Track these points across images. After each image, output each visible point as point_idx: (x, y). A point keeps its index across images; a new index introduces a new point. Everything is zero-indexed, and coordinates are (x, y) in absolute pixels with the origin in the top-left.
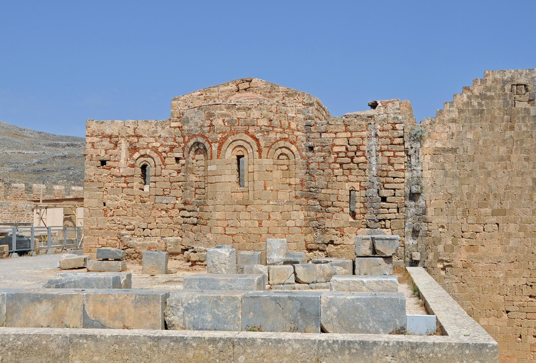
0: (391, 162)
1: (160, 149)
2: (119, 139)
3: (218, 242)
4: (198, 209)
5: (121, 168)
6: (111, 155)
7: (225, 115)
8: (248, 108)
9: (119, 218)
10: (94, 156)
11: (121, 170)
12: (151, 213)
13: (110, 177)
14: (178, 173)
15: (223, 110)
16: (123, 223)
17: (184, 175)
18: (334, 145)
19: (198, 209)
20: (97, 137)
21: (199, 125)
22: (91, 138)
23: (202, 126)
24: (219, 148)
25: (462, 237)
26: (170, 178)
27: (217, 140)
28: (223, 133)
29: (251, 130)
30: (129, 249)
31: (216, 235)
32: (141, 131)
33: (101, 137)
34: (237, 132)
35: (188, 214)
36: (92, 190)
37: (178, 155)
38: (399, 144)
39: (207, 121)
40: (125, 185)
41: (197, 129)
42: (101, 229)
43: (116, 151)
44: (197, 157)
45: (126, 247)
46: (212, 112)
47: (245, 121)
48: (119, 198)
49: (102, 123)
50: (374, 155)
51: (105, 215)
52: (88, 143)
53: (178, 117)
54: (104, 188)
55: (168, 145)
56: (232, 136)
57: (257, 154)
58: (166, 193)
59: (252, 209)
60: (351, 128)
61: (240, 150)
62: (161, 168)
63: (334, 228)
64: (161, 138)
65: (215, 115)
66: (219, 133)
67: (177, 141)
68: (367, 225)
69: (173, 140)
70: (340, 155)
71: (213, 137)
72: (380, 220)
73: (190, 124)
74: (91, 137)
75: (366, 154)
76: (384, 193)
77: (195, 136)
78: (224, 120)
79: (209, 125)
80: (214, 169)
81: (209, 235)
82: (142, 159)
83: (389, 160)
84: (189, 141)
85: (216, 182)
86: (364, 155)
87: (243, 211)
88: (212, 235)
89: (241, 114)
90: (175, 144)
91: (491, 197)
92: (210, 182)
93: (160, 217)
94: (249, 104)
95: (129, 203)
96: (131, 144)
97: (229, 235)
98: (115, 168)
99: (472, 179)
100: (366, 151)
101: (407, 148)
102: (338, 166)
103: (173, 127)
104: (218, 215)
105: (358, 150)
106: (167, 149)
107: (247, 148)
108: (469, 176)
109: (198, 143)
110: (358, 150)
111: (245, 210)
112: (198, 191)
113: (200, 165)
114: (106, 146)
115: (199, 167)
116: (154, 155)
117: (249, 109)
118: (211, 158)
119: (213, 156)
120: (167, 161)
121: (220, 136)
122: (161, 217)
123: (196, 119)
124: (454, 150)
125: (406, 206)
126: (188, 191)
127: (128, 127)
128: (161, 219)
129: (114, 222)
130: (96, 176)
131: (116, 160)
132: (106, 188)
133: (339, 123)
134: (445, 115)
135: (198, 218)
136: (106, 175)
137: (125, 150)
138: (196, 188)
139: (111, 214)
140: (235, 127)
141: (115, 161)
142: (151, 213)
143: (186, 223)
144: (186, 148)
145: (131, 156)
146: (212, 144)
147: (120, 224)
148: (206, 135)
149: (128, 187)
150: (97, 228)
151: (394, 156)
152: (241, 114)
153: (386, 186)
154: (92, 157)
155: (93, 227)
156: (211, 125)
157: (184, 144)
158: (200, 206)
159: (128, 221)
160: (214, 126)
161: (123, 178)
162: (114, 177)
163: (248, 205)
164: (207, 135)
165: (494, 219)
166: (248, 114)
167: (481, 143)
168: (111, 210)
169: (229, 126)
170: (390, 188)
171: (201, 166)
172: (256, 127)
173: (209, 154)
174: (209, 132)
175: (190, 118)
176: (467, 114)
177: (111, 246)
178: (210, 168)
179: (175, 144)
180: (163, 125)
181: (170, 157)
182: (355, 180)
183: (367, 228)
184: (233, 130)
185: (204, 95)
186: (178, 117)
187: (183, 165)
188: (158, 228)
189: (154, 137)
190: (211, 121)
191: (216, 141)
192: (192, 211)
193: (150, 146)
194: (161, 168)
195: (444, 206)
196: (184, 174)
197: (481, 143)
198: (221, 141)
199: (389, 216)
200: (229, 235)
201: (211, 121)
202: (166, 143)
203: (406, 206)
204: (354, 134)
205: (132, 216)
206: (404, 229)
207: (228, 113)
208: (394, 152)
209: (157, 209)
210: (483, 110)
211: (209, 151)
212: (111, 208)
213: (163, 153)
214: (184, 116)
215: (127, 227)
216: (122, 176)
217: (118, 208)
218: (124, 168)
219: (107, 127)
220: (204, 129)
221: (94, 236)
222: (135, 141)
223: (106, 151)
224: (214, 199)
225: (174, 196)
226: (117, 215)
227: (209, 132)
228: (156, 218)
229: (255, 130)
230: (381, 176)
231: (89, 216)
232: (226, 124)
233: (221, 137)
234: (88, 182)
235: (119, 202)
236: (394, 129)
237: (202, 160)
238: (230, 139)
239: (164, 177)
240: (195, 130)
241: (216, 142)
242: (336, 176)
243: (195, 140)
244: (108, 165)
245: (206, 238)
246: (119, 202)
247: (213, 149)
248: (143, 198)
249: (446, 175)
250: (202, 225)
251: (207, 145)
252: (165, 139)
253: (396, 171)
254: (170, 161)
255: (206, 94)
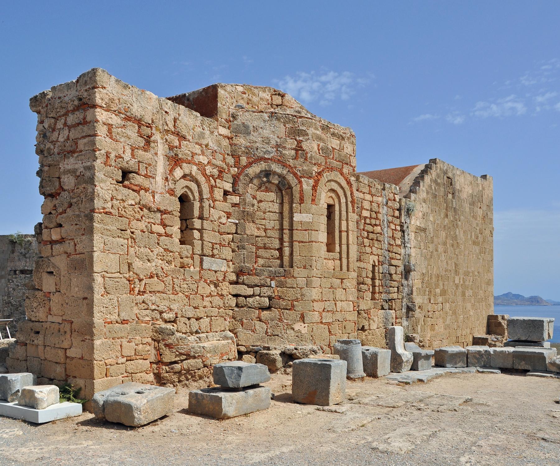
0: (395, 235)
1: (209, 170)
2: (154, 131)
3: (314, 336)
4: (273, 283)
5: (157, 192)
6: (139, 162)
7: (319, 139)
8: (341, 136)
9: (153, 298)
10: (112, 156)
11: (156, 197)
12: (198, 287)
13: (139, 209)
14: (228, 218)
15: (318, 130)
16: (160, 309)
17: (236, 224)
18: (362, 208)
19: (273, 283)
20: (116, 115)
21: (273, 142)
22: (106, 113)
23: (278, 146)
24: (314, 188)
25: (428, 317)
26: (219, 226)
27: (312, 174)
28: (319, 165)
29: (345, 171)
30: (191, 361)
31: (312, 324)
32: (184, 127)
33: (123, 116)
34: (332, 169)
35: (250, 291)
36: (109, 233)
37: (228, 187)
38: (397, 217)
39: (289, 140)
40: (160, 229)
41: (270, 149)
42: (124, 322)
43: (147, 156)
44: (260, 195)
45: (185, 357)
46: (301, 128)
47: (340, 155)
48: (153, 256)
49: (126, 87)
50: (386, 226)
51: (132, 290)
52: (101, 122)
53: (226, 120)
54: (129, 231)
55: (217, 166)
56: (327, 173)
57: (350, 205)
58: (216, 252)
59: (348, 284)
60: (373, 191)
61: (331, 197)
62: (210, 205)
63: (364, 310)
64: (208, 149)
65: (307, 135)
66: (315, 164)
67: (227, 161)
68: (382, 306)
69: (221, 157)
70: (368, 221)
71: (305, 168)
72: (389, 300)
73: (251, 137)
74: (106, 111)
75: (381, 223)
76: (393, 271)
77: (266, 160)
78: (319, 146)
79: (294, 146)
80: (308, 220)
81: (298, 326)
82: (184, 183)
83: (393, 234)
84: (250, 165)
85: (312, 242)
86: (380, 225)
87: (339, 288)
88: (306, 325)
89: (335, 143)
90: (225, 166)
91: (440, 278)
92: (299, 240)
93: (209, 296)
94: (342, 131)
95: (166, 267)
96: (171, 148)
97: (325, 324)
98: (146, 190)
99: (432, 259)
100: (382, 221)
101: (402, 223)
102: (366, 234)
103: (221, 135)
104: (314, 293)
105: (377, 218)
106: (216, 172)
107: (340, 195)
108: (431, 258)
109: (268, 173)
110: (377, 218)
111: (340, 287)
112: (261, 252)
113: (268, 210)
114: (132, 140)
115: (264, 213)
116: (202, 179)
117: (343, 139)
118: (302, 200)
119: (305, 199)
120: (216, 190)
121: (315, 169)
122: (210, 295)
123: (264, 131)
124: (424, 230)
125: (402, 286)
126: (245, 252)
127: (166, 112)
128: (209, 299)
129: (146, 307)
130: (115, 202)
131: (149, 174)
132: (132, 233)
133: (366, 182)
134: (421, 194)
135: (270, 298)
136: (134, 203)
137: (161, 158)
138: (258, 248)
139: (142, 289)
140: (329, 160)
141: (146, 176)
142: (198, 287)
143: (242, 307)
144: (241, 177)
145: (171, 171)
146: (302, 179)
147: (155, 310)
148: (288, 163)
149: (167, 235)
150: (119, 321)
151: (396, 230)
152: (335, 143)
153: (394, 262)
154: (108, 157)
155: (112, 317)
156: (299, 148)
157: (236, 169)
158: (277, 278)
159: (167, 303)
160: (304, 151)
161: (159, 215)
162: (144, 209)
163: (344, 279)
164: (291, 162)
165: (440, 299)
166: (342, 145)
167: (436, 225)
168: (140, 280)
169: (324, 156)
170: (394, 264)
171: (269, 212)
172: (350, 167)
173: (297, 196)
174: (296, 158)
175: (251, 128)
176: (430, 196)
177: (142, 357)
178: (297, 217)
179: (225, 166)
180: (211, 127)
181: (219, 188)
182: (376, 253)
183: (381, 309)
184: (328, 164)
185: (247, 95)
186: (226, 120)
187: (234, 205)
188: (207, 316)
189: (201, 145)
190: (299, 142)
191: (310, 175)
192: (258, 286)
193: (197, 159)
194: (210, 205)
195: (420, 287)
196: (237, 222)
197: (436, 225)
198: (316, 178)
199: (395, 296)
200: (325, 324)
201: (299, 142)
202: (214, 161)
203: (402, 286)
204: (375, 198)
205: (173, 294)
206: (402, 310)
207: (323, 136)
208: (395, 225)
209: (205, 281)
210: (436, 195)
211: (296, 190)
212: (142, 277)
213: (211, 178)
214: (239, 120)
215: (165, 316)
216: (159, 210)
217: (151, 277)
218: (161, 193)
219: (134, 99)
220: (284, 152)
221: (113, 339)
222: (175, 144)
223: (133, 151)
224: (308, 267)
225: (224, 258)
226: (150, 292)
227: (296, 158)
228: (204, 298)
229: (349, 171)
230: (389, 251)
231: (103, 293)
232: (321, 152)
233: (316, 171)
234: (100, 213)
235: (154, 264)
236: (394, 200)
237: (273, 201)
238: (326, 176)
239: (212, 221)
240: (263, 149)
241: (310, 178)
242: (365, 246)
243: (263, 166)
244: (137, 183)
245: (292, 331)
246: (154, 264)
247: (305, 186)
248: (182, 258)
249: (421, 254)
250: (284, 309)
251: (290, 178)
252: (214, 152)
253: (396, 246)
254: (218, 194)
255: (249, 95)
